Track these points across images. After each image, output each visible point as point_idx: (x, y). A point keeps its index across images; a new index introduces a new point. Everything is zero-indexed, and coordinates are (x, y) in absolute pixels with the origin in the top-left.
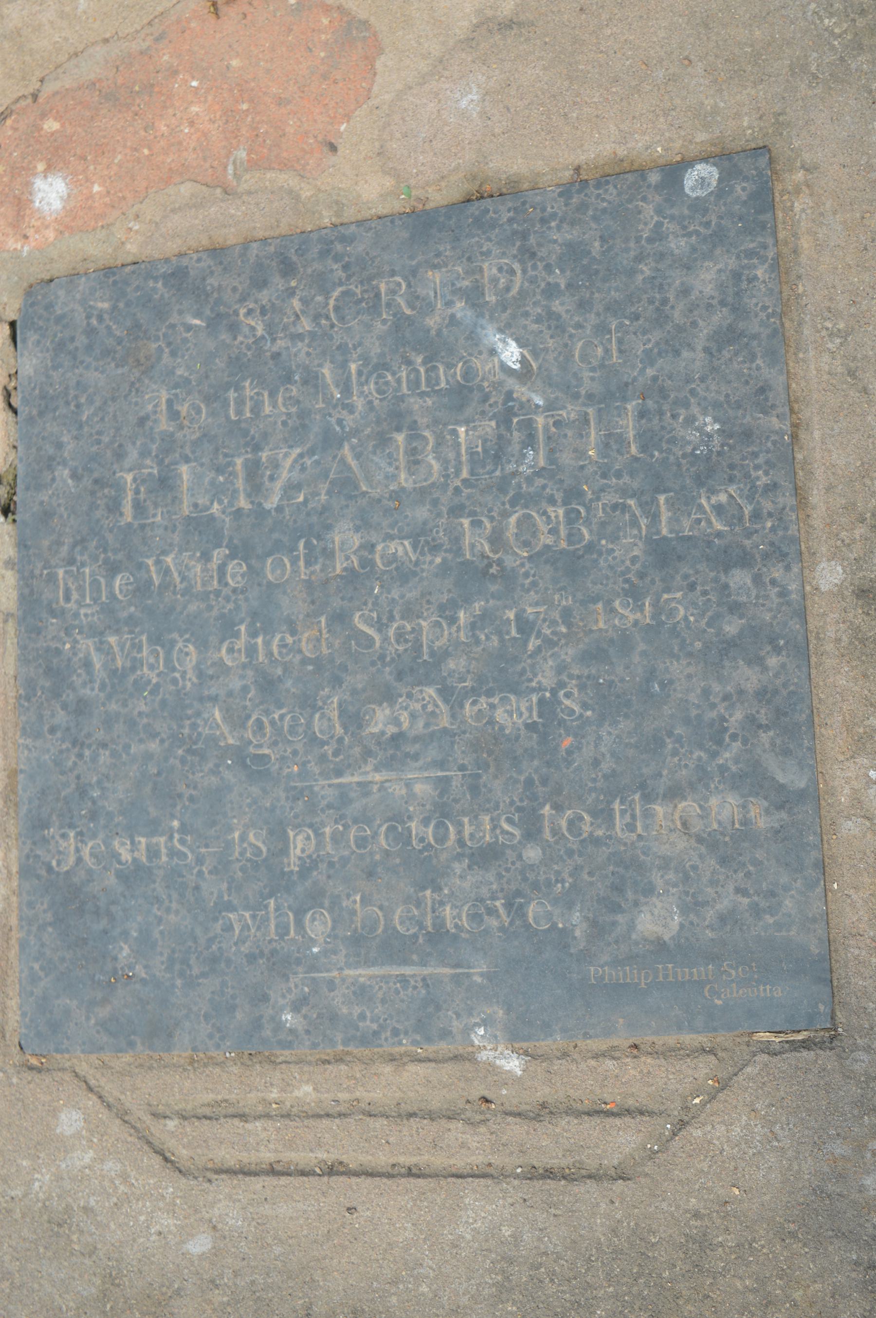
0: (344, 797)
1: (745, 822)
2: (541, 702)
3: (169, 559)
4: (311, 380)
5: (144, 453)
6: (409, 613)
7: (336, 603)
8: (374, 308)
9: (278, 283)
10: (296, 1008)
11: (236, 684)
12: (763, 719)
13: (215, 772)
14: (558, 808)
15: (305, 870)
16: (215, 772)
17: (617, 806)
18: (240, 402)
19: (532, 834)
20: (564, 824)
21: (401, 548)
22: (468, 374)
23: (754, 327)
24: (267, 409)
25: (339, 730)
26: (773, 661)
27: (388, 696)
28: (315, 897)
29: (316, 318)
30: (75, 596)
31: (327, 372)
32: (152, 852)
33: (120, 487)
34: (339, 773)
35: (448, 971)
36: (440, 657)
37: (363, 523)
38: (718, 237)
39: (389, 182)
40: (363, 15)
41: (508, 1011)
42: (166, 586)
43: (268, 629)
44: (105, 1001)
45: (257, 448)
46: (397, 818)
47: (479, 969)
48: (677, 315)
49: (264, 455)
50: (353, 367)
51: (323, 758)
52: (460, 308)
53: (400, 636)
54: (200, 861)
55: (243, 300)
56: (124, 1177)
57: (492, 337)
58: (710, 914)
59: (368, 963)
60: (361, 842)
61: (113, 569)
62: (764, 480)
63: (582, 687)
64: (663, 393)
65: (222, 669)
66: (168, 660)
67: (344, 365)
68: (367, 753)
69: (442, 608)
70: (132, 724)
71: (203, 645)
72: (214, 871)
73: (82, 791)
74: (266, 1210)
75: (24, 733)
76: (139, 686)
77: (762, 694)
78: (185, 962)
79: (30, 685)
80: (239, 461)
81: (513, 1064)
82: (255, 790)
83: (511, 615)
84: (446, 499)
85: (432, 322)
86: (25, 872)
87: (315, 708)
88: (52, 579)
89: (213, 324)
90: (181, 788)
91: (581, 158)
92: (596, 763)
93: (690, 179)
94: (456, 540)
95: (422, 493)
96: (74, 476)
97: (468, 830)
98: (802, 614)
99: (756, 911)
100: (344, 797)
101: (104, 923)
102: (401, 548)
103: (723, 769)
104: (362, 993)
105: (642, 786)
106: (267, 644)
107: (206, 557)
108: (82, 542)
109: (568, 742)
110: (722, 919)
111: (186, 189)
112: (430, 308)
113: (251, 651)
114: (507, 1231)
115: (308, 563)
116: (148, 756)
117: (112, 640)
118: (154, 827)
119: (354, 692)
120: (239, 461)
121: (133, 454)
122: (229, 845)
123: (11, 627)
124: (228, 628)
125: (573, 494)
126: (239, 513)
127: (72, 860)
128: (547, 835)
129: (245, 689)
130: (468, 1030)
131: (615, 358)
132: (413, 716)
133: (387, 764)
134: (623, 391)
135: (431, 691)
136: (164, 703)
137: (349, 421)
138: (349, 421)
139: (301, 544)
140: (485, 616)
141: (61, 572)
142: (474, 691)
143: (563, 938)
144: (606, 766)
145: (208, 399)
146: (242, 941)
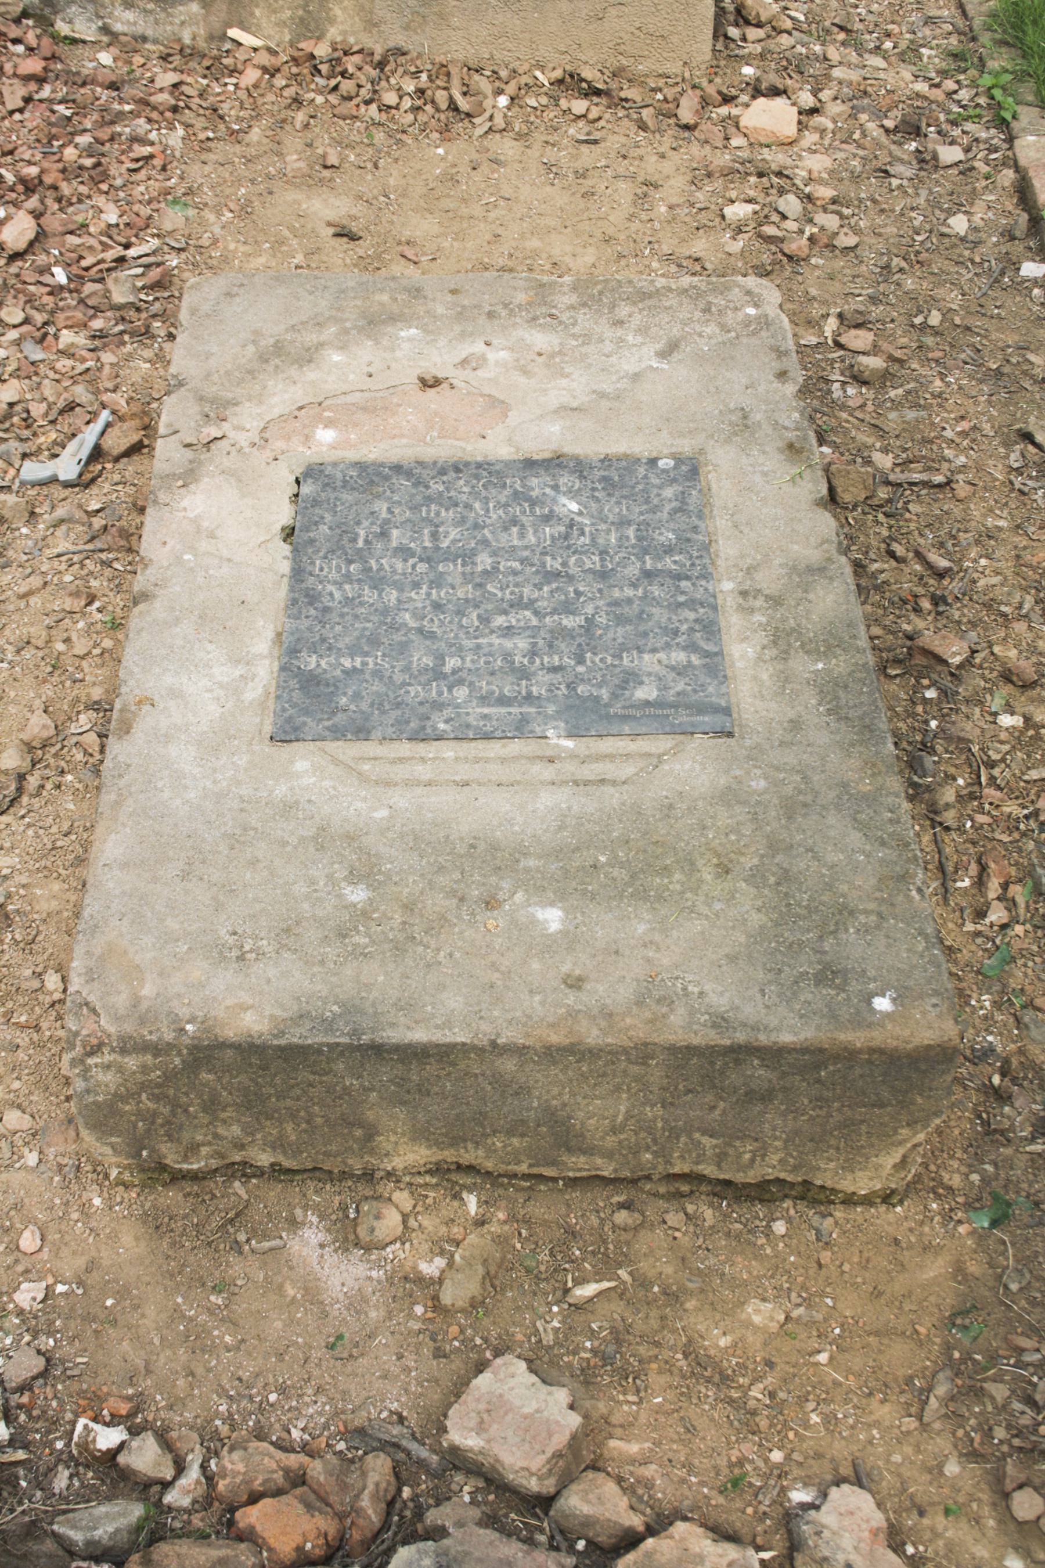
0: (479, 647)
1: (689, 662)
2: (586, 619)
3: (383, 561)
4: (468, 506)
5: (372, 524)
6: (517, 585)
7: (478, 580)
8: (504, 486)
9: (452, 474)
10: (446, 722)
11: (420, 605)
12: (697, 627)
13: (405, 635)
14: (595, 654)
15: (454, 672)
16: (405, 635)
17: (625, 655)
18: (428, 512)
19: (581, 660)
20: (597, 660)
21: (516, 565)
22: (551, 511)
23: (691, 508)
24: (443, 513)
25: (476, 623)
26: (702, 611)
27: (505, 612)
28: (461, 682)
29: (473, 487)
30: (326, 570)
31: (477, 505)
32: (365, 664)
33: (357, 535)
34: (476, 638)
35: (533, 710)
36: (532, 602)
37: (494, 554)
38: (674, 481)
39: (512, 450)
40: (502, 398)
41: (567, 723)
42: (381, 568)
43: (439, 586)
44: (329, 719)
45: (437, 526)
46: (507, 656)
47: (551, 709)
48: (656, 501)
49: (441, 530)
50: (491, 505)
51: (468, 633)
52: (548, 491)
53: (512, 593)
54: (393, 667)
55: (433, 478)
56: (334, 788)
57: (563, 500)
58: (672, 692)
59: (489, 705)
60: (487, 663)
61: (350, 562)
62: (695, 554)
63: (607, 614)
64: (648, 525)
65: (411, 599)
66: (380, 595)
67: (487, 503)
68: (492, 632)
69: (535, 585)
70: (356, 617)
71: (401, 590)
72: (402, 671)
73: (323, 640)
74: (424, 799)
75: (289, 617)
76: (362, 604)
77: (696, 621)
78: (381, 704)
79: (294, 602)
80: (426, 531)
81: (569, 744)
82: (428, 643)
83: (571, 589)
84: (538, 550)
85: (534, 494)
86: (283, 669)
87: (464, 615)
88: (313, 563)
89: (416, 485)
90: (385, 640)
91: (609, 452)
92: (614, 639)
93: (661, 463)
94: (543, 564)
95: (526, 547)
96: (330, 528)
97: (546, 659)
98: (714, 596)
99: (695, 691)
100: (479, 647)
101: (332, 689)
102: (516, 565)
103: (678, 644)
104: (485, 717)
105: (638, 648)
106: (438, 593)
107: (405, 560)
108: (333, 552)
109: (600, 632)
110: (678, 694)
111: (404, 441)
112: (533, 489)
113: (429, 594)
114: (564, 806)
115: (463, 566)
116: (365, 629)
117: (347, 587)
118: (366, 654)
119: (486, 611)
120: (426, 531)
121: (366, 524)
122: (411, 662)
123: (286, 580)
124: (416, 585)
125: (603, 553)
126: (425, 548)
127: (313, 666)
128: (588, 663)
129: (424, 607)
130: (544, 731)
131: (625, 512)
132: (518, 620)
133: (504, 636)
134: (629, 523)
135: (528, 613)
136: (376, 610)
137: (488, 521)
138: (488, 521)
139: (460, 561)
140: (557, 589)
141: (318, 562)
142: (552, 614)
143: (597, 699)
144: (620, 640)
145: (411, 509)
146: (416, 696)
